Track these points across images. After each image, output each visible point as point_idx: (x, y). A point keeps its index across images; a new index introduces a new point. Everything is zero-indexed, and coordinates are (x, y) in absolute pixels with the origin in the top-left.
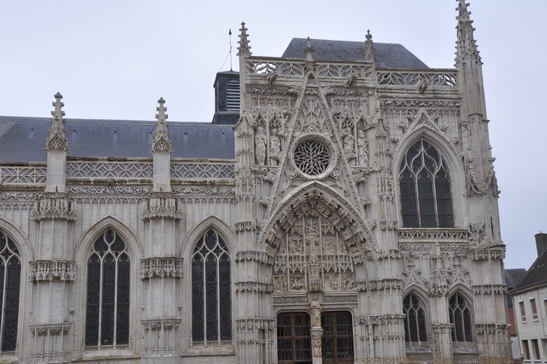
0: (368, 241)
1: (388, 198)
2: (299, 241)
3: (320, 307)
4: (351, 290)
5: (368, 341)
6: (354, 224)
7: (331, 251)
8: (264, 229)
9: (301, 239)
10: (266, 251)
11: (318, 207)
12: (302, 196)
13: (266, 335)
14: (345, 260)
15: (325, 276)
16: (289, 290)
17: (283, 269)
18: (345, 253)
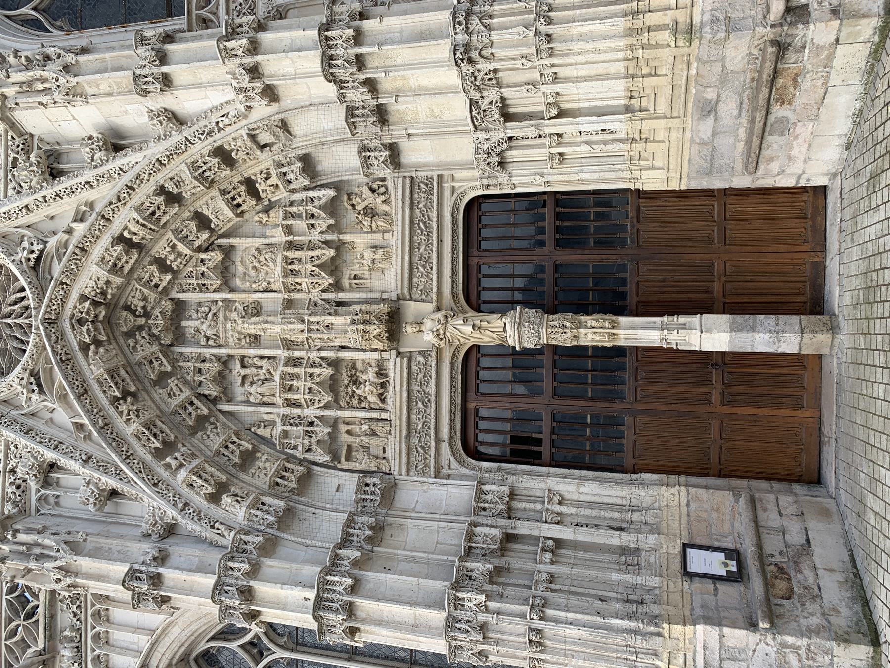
0: (219, 139)
1: (66, 68)
2: (243, 366)
3: (440, 315)
4: (392, 198)
5: (566, 139)
6: (170, 187)
7: (271, 264)
8: (171, 513)
9: (238, 363)
10: (244, 509)
11: (141, 304)
12: (89, 365)
13: (523, 528)
14: (299, 216)
15: (351, 289)
16: (385, 415)
17: (323, 431)
18: (276, 216)
